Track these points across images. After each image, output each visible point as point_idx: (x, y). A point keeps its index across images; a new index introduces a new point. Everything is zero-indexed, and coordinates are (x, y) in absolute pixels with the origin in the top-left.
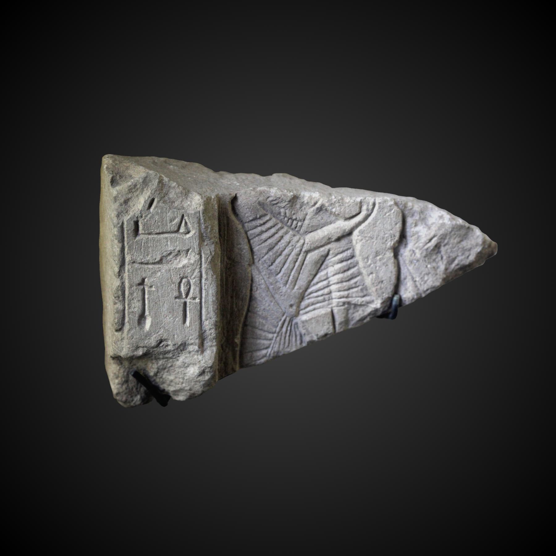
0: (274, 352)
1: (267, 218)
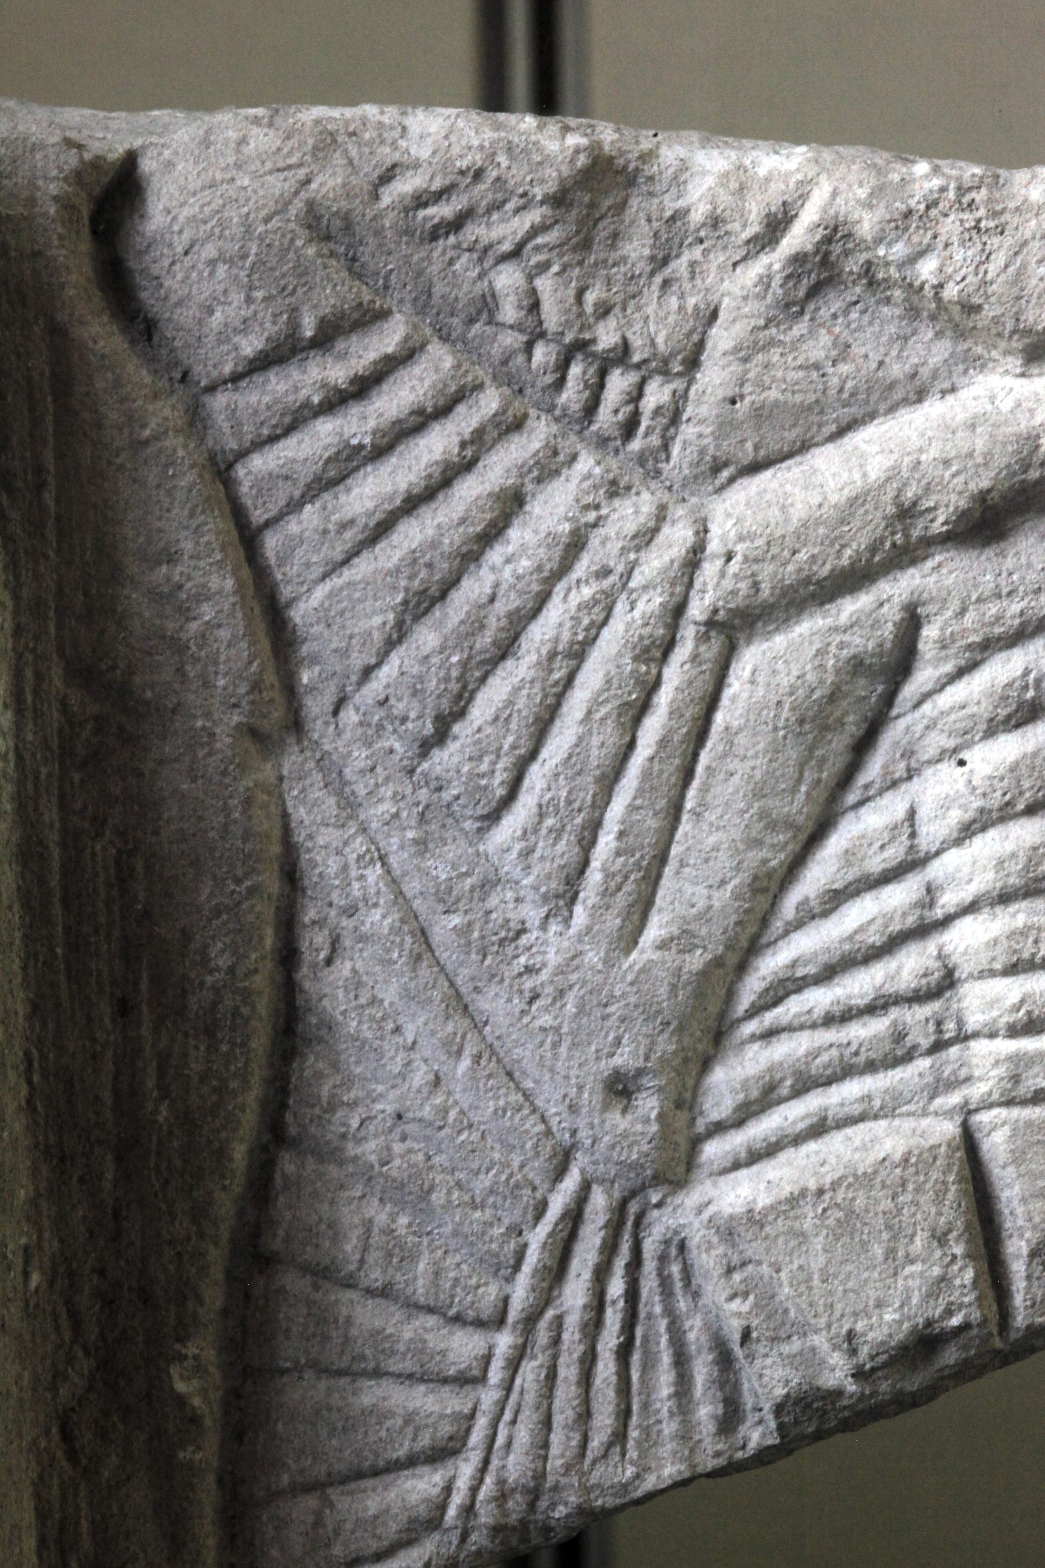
0: (502, 1496)
1: (389, 338)
